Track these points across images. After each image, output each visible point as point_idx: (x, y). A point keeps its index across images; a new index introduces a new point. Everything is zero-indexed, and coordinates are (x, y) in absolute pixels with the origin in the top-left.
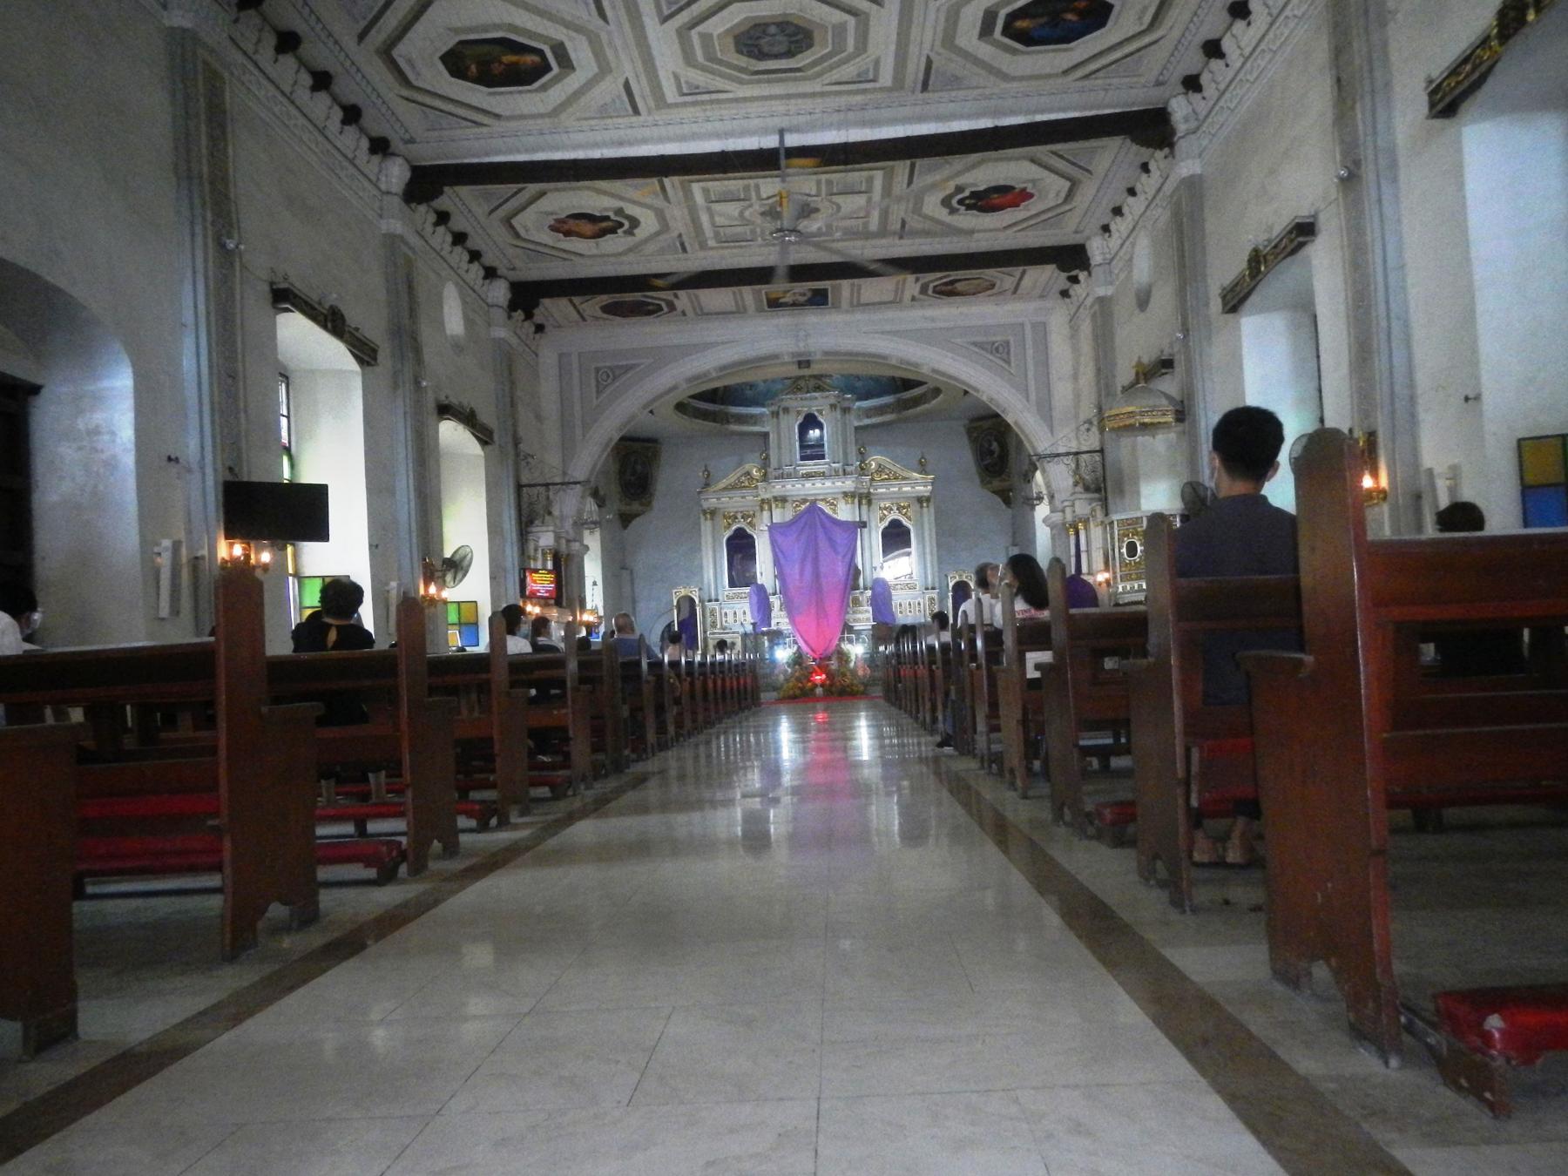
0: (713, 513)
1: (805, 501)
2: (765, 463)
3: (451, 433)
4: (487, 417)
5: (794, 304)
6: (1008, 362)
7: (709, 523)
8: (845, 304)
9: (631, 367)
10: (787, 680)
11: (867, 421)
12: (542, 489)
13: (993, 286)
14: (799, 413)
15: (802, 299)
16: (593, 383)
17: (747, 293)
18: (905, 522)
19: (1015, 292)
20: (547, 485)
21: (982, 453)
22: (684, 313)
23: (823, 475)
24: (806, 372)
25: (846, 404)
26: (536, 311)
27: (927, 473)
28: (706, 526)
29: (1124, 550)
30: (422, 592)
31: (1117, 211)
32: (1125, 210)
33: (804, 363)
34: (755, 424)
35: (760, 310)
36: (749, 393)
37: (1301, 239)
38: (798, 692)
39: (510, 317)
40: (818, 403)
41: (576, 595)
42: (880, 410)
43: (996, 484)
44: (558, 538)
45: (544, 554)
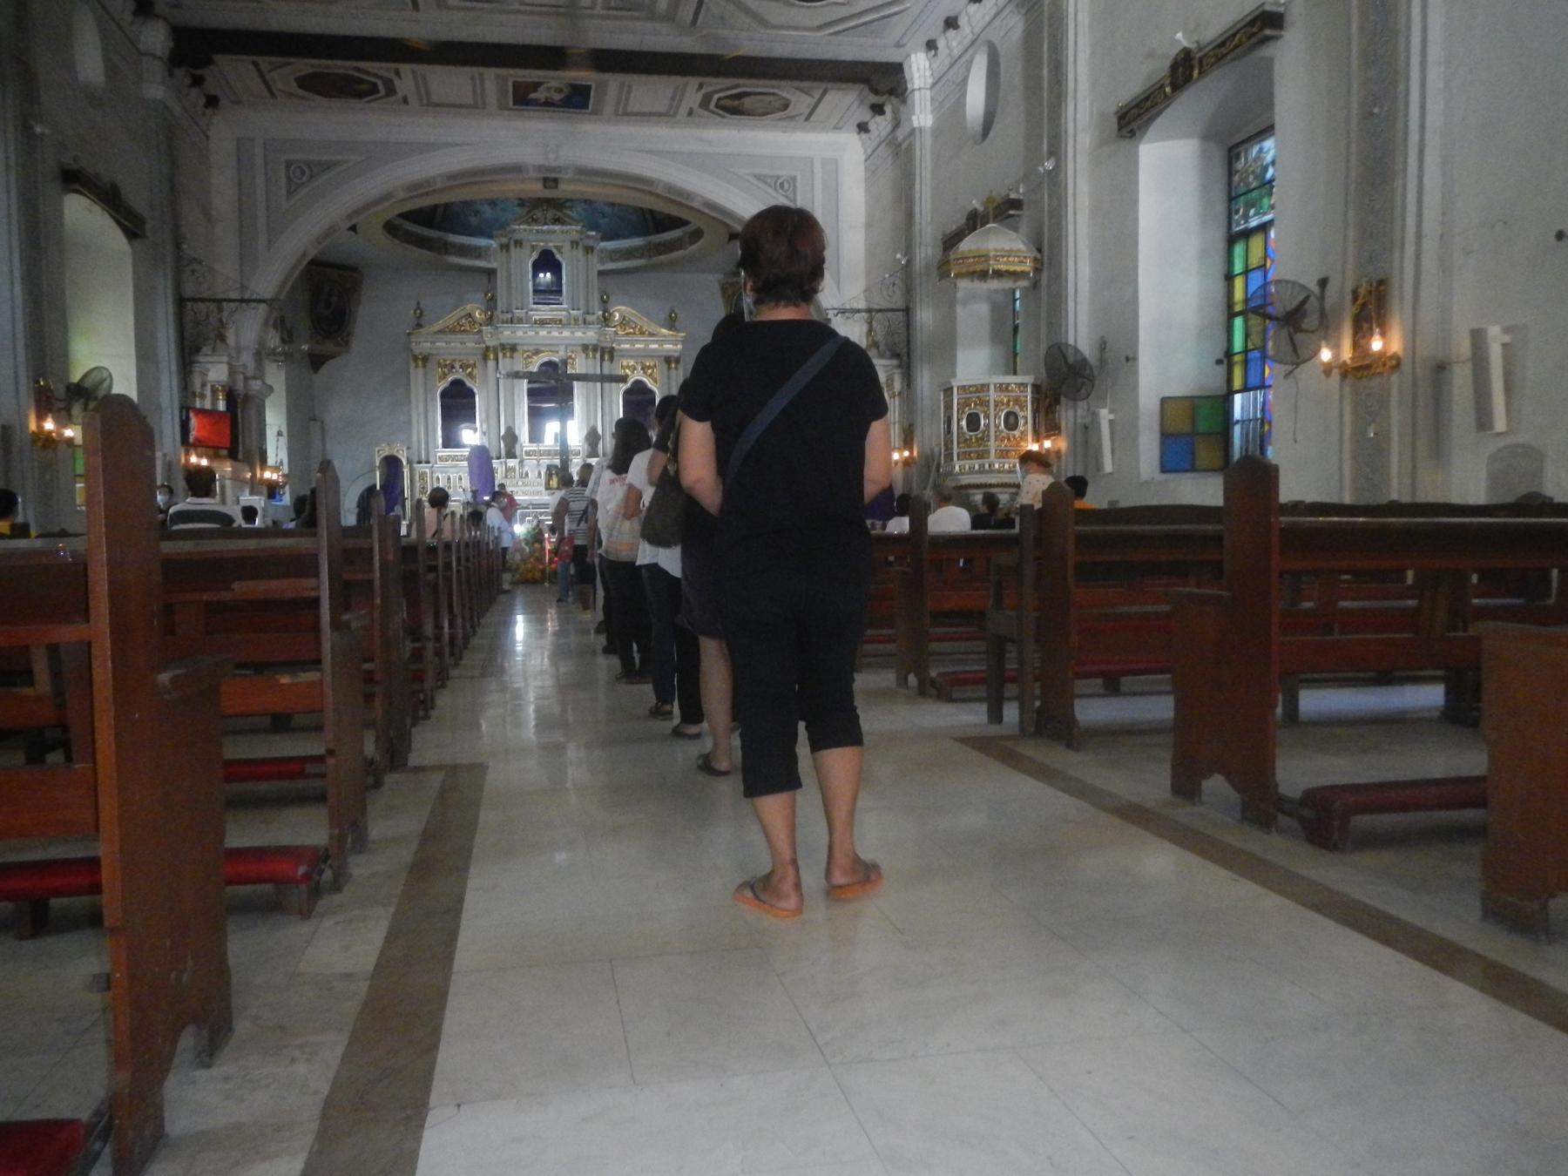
0: (425, 359)
1: (537, 352)
2: (491, 305)
3: (81, 215)
4: (137, 199)
5: (548, 104)
7: (420, 370)
8: (609, 108)
9: (335, 164)
10: (524, 561)
12: (212, 306)
13: (786, 106)
15: (557, 97)
16: (283, 181)
17: (490, 74)
18: (650, 384)
19: (807, 119)
20: (219, 301)
22: (405, 101)
23: (558, 322)
24: (549, 194)
25: (590, 243)
26: (205, 72)
27: (677, 330)
28: (417, 374)
29: (964, 423)
30: (33, 426)
31: (951, 23)
32: (962, 21)
33: (551, 182)
34: (479, 257)
35: (502, 107)
36: (474, 220)
37: (1268, 32)
38: (538, 575)
39: (171, 75)
40: (557, 237)
41: (254, 445)
42: (629, 254)
44: (232, 372)
45: (214, 392)
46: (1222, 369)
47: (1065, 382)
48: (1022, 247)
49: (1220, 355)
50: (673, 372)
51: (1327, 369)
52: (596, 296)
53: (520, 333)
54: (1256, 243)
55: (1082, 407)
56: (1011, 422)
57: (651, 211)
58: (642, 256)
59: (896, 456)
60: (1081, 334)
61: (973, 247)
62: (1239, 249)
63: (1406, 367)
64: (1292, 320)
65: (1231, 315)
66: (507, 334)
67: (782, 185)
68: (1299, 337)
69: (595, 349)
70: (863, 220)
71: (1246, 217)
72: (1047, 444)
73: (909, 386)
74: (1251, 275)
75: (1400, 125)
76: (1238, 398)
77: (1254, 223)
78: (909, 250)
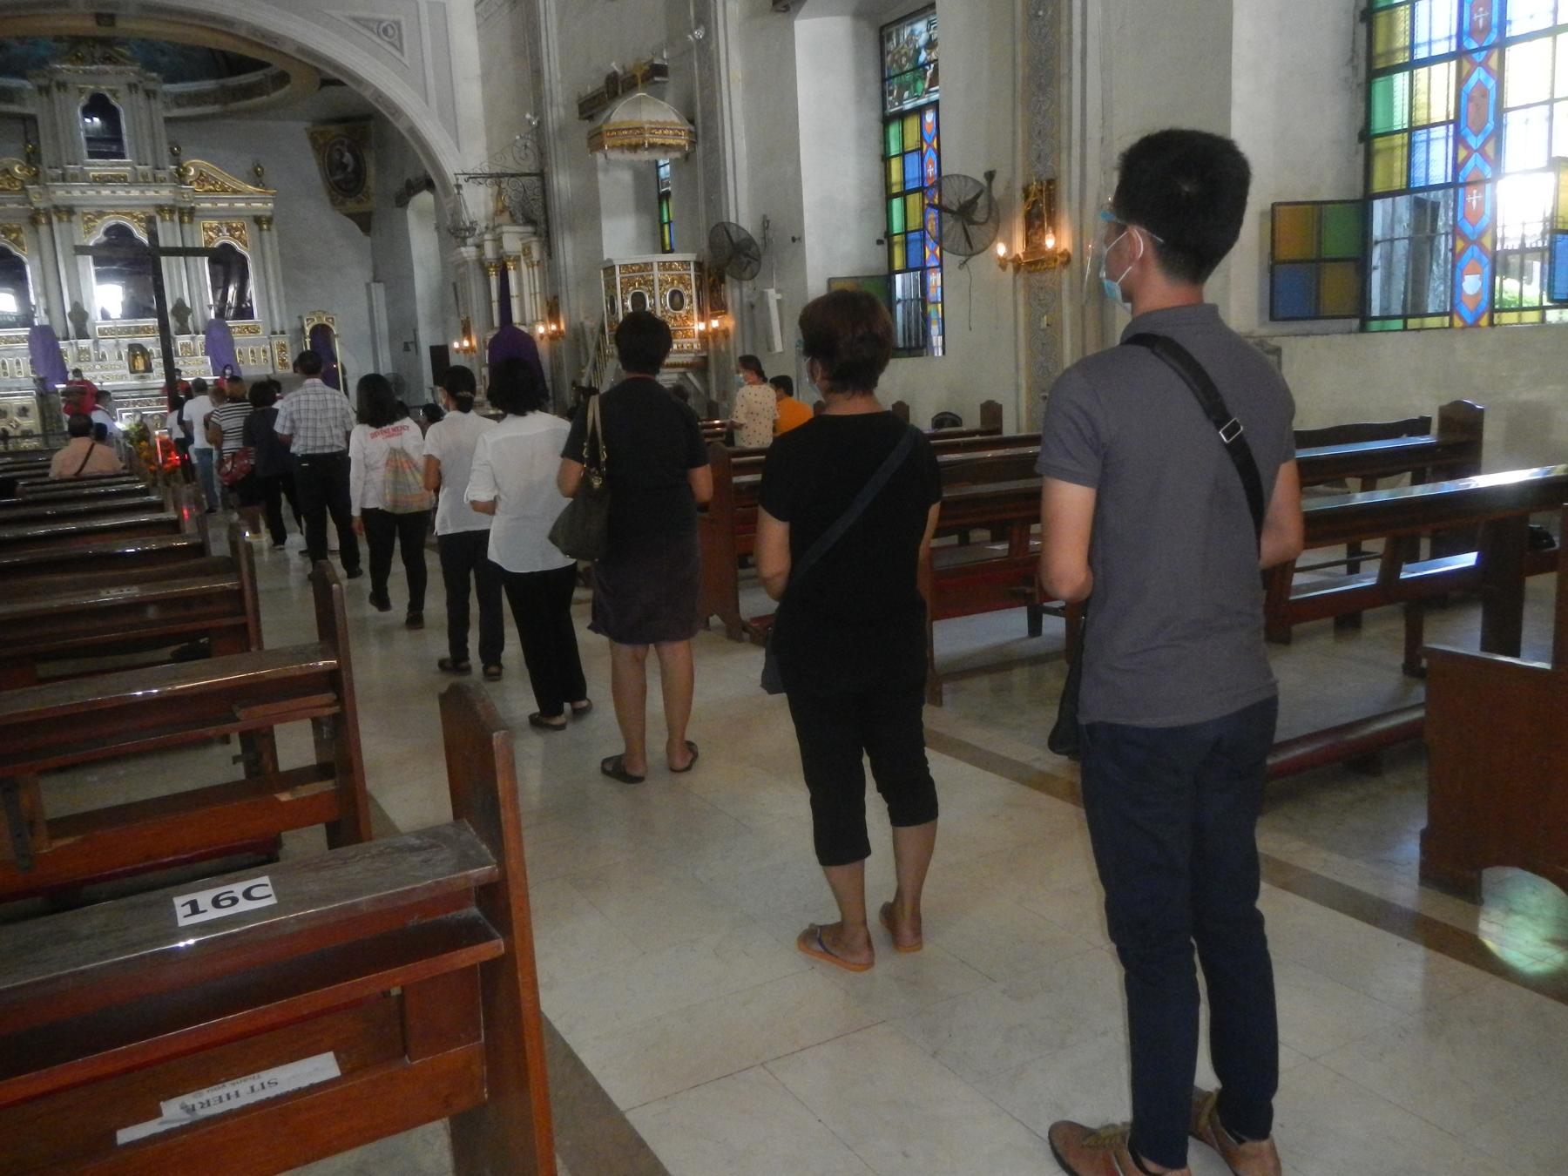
1: (101, 214)
2: (33, 158)
6: (400, 49)
11: (177, 112)
14: (81, 91)
21: (331, 167)
24: (103, 32)
25: (151, 86)
29: (629, 303)
34: (11, 101)
40: (112, 80)
43: (351, 205)
46: (883, 249)
47: (729, 261)
48: (673, 118)
49: (881, 237)
50: (265, 233)
51: (1003, 263)
52: (166, 148)
53: (76, 193)
54: (912, 124)
55: (747, 287)
56: (677, 300)
57: (223, 53)
58: (215, 103)
59: (541, 329)
60: (742, 211)
61: (626, 118)
62: (894, 130)
63: (1075, 264)
64: (965, 212)
65: (889, 197)
66: (60, 194)
67: (385, 31)
68: (972, 229)
69: (171, 212)
70: (479, 72)
71: (901, 100)
72: (715, 324)
73: (550, 255)
74: (908, 158)
75: (1064, 28)
76: (898, 278)
77: (908, 106)
78: (539, 111)
